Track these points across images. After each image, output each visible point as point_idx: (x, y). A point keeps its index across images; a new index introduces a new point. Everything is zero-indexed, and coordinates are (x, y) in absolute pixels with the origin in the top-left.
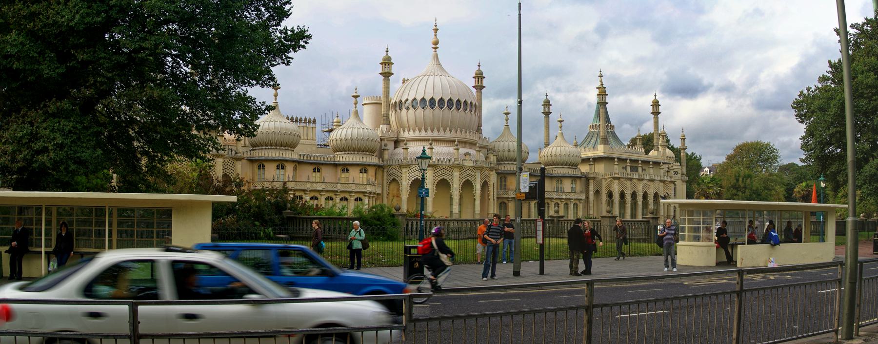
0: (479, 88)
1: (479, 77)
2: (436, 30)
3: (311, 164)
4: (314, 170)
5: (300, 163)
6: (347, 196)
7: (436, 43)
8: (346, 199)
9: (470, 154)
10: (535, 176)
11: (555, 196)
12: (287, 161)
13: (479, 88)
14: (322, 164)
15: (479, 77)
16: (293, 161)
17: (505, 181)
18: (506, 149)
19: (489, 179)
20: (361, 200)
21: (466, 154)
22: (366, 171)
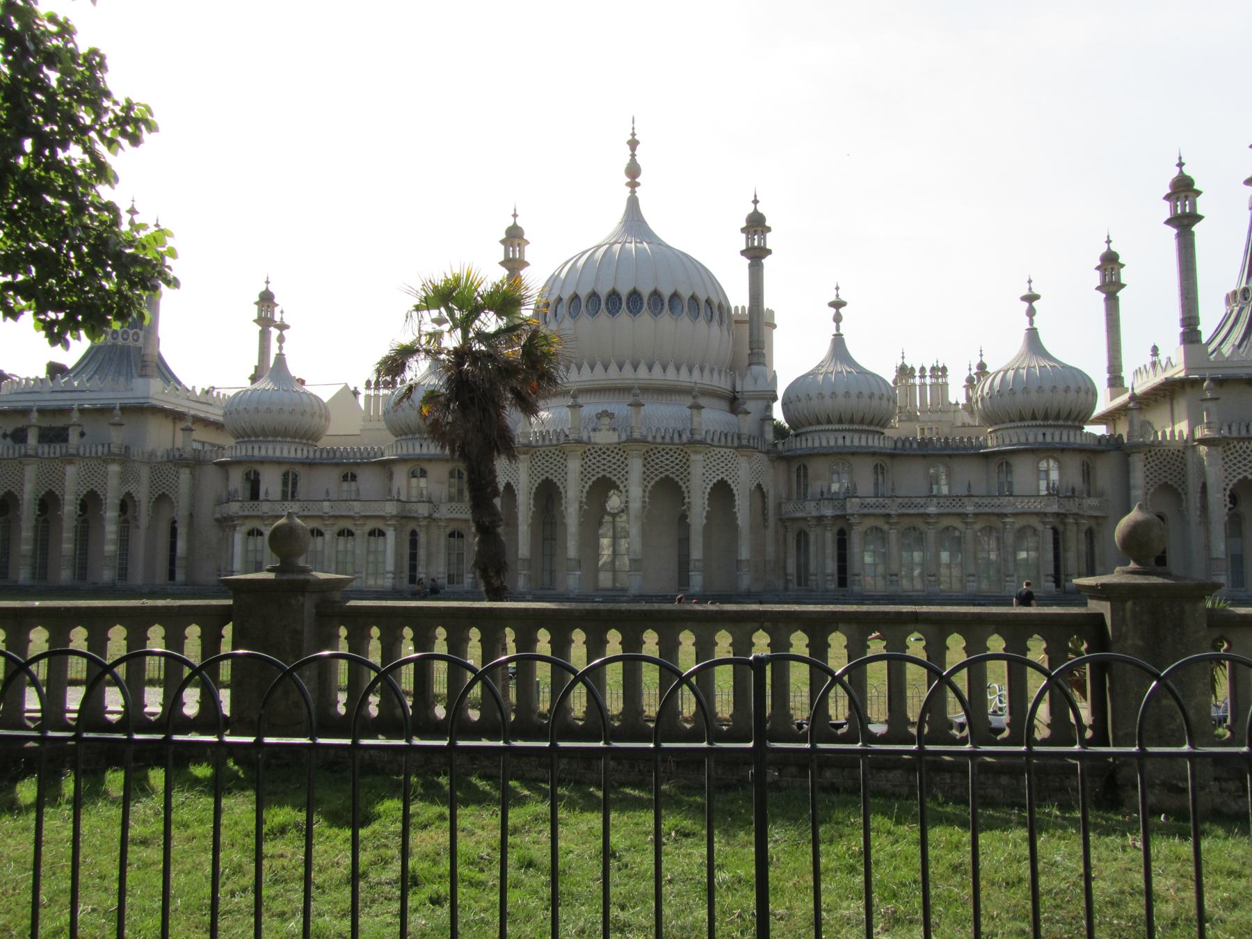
0: (756, 255)
1: (756, 225)
2: (633, 144)
3: (337, 465)
4: (345, 478)
5: (310, 464)
6: (348, 525)
7: (633, 171)
8: (350, 533)
9: (611, 416)
10: (924, 456)
11: (932, 510)
12: (262, 462)
13: (756, 255)
14: (358, 464)
15: (756, 225)
16: (278, 462)
17: (806, 476)
18: (866, 393)
19: (687, 476)
20: (382, 534)
21: (600, 416)
22: (423, 474)
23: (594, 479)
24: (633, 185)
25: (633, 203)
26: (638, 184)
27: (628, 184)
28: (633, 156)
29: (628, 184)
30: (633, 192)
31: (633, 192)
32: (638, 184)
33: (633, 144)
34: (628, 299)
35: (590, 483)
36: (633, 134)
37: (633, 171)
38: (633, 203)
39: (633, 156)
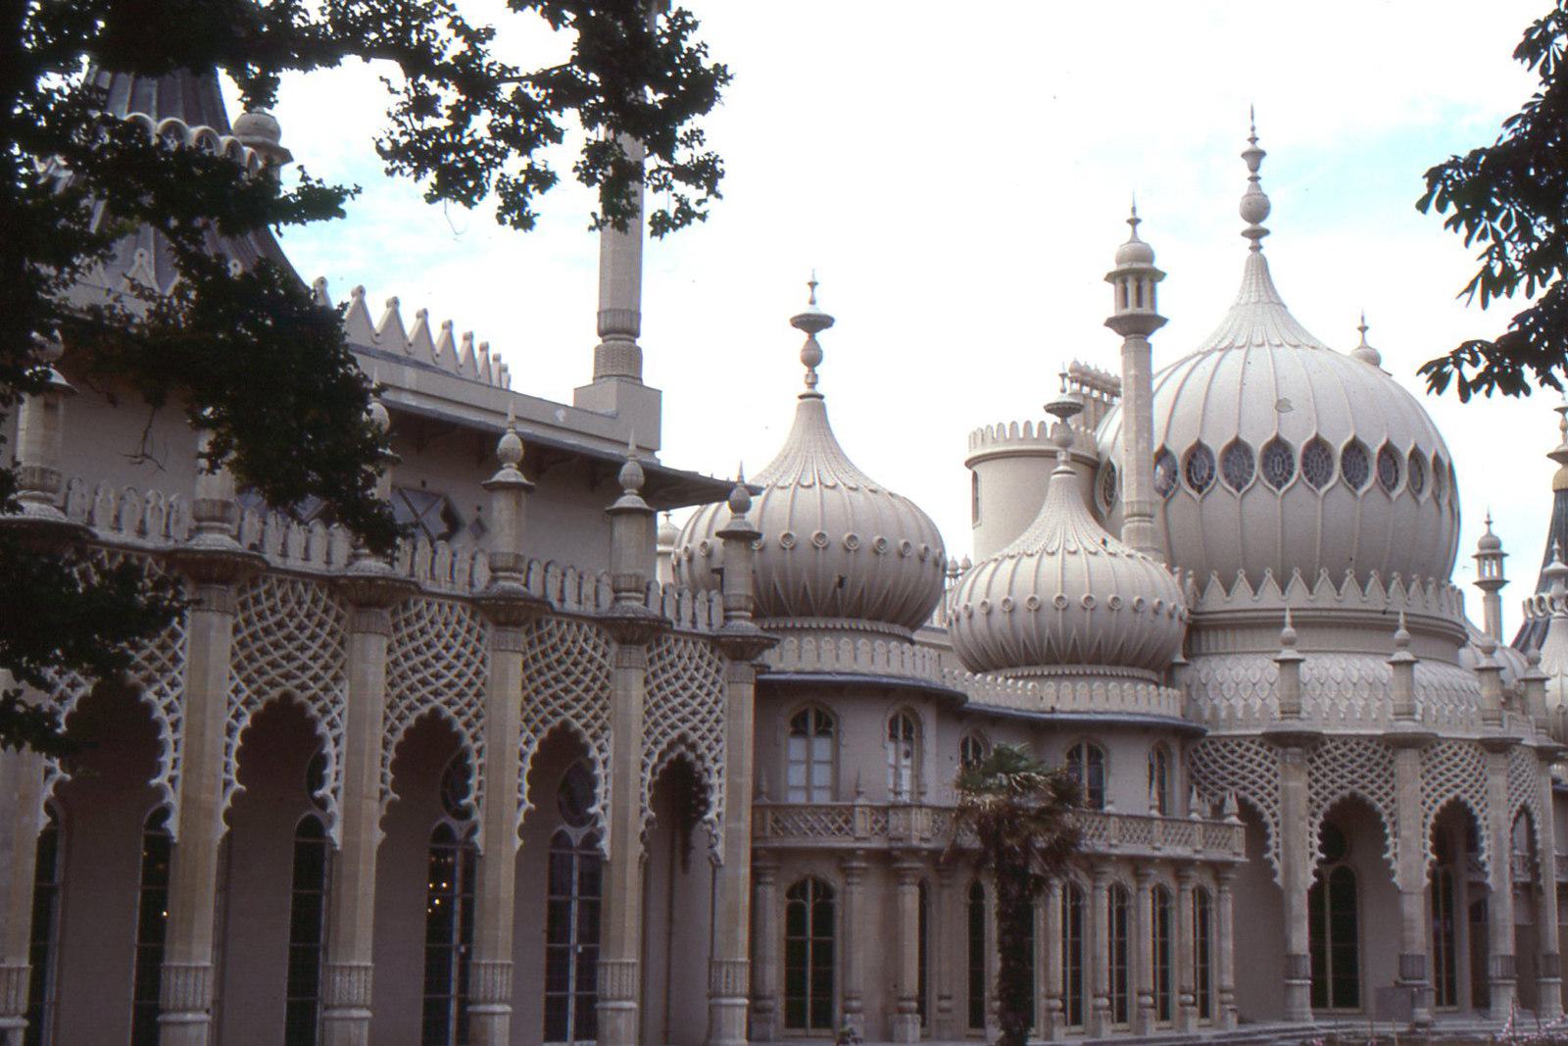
2: (1255, 157)
7: (1256, 212)
23: (1443, 802)
24: (1256, 235)
25: (1260, 269)
26: (1266, 232)
27: (1244, 234)
28: (1255, 179)
29: (1244, 234)
30: (1256, 248)
31: (1256, 248)
32: (1266, 232)
33: (1255, 157)
34: (1344, 458)
35: (1437, 808)
36: (1253, 140)
37: (1256, 212)
38: (1260, 269)
39: (1255, 179)
